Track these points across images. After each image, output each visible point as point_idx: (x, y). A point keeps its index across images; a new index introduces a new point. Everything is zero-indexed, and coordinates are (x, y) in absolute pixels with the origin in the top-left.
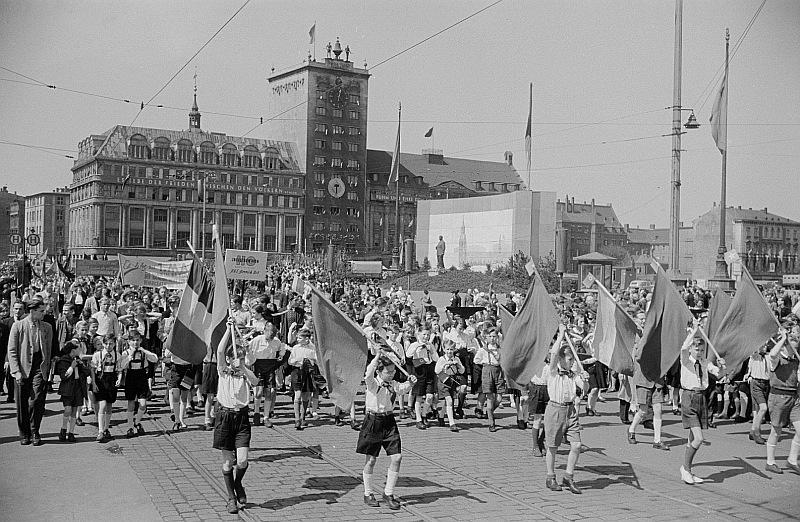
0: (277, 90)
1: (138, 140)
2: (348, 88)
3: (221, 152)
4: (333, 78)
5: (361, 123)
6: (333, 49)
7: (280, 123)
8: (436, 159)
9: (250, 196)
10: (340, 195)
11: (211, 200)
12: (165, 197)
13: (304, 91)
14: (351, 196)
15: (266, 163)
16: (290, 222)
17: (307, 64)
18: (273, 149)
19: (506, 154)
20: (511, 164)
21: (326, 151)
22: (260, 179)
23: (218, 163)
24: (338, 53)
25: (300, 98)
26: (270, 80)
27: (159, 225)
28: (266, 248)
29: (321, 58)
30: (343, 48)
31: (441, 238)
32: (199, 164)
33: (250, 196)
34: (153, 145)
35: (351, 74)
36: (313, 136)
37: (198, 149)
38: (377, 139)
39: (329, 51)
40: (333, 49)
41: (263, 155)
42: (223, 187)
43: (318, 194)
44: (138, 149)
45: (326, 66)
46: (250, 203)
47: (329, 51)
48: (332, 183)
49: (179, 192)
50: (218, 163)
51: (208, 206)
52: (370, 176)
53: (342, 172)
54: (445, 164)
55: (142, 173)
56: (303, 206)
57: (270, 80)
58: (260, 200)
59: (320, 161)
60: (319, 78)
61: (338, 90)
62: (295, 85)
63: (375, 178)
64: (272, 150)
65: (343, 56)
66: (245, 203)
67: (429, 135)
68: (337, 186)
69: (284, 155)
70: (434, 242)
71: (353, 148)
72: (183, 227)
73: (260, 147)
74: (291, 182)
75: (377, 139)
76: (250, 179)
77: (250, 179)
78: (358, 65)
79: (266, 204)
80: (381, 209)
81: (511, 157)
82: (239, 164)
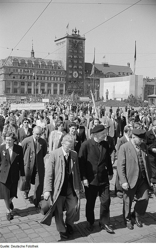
0: (57, 44)
1: (15, 60)
2: (79, 43)
3: (40, 64)
4: (74, 40)
5: (83, 54)
6: (74, 31)
8: (106, 65)
9: (49, 77)
10: (77, 77)
11: (38, 79)
12: (24, 78)
13: (65, 44)
14: (80, 77)
15: (53, 67)
16: (61, 85)
17: (66, 36)
18: (56, 63)
20: (129, 67)
21: (73, 64)
22: (52, 72)
23: (40, 67)
24: (76, 32)
25: (64, 47)
26: (55, 41)
27: (22, 87)
28: (54, 93)
29: (70, 34)
30: (77, 30)
31: (107, 90)
32: (34, 68)
33: (49, 77)
34: (20, 62)
35: (80, 39)
36: (68, 59)
37: (34, 63)
38: (88, 59)
39: (73, 32)
40: (74, 31)
41: (53, 65)
42: (41, 75)
43: (70, 77)
44: (15, 64)
46: (49, 80)
47: (73, 32)
48: (74, 73)
49: (28, 77)
50: (40, 67)
51: (37, 81)
52: (86, 71)
53: (77, 69)
54: (109, 67)
55: (17, 71)
56: (65, 81)
57: (55, 41)
58: (52, 79)
59: (70, 66)
60: (70, 40)
61: (76, 44)
62: (63, 43)
63: (87, 72)
64: (56, 63)
65: (77, 33)
66: (48, 79)
67: (104, 57)
68: (75, 74)
69: (59, 64)
70: (105, 91)
71: (80, 62)
72: (29, 87)
73: (52, 62)
74: (62, 73)
75: (88, 59)
76: (49, 72)
77: (49, 72)
78: (82, 36)
79: (54, 80)
80: (89, 81)
81: (129, 64)
82: (46, 68)
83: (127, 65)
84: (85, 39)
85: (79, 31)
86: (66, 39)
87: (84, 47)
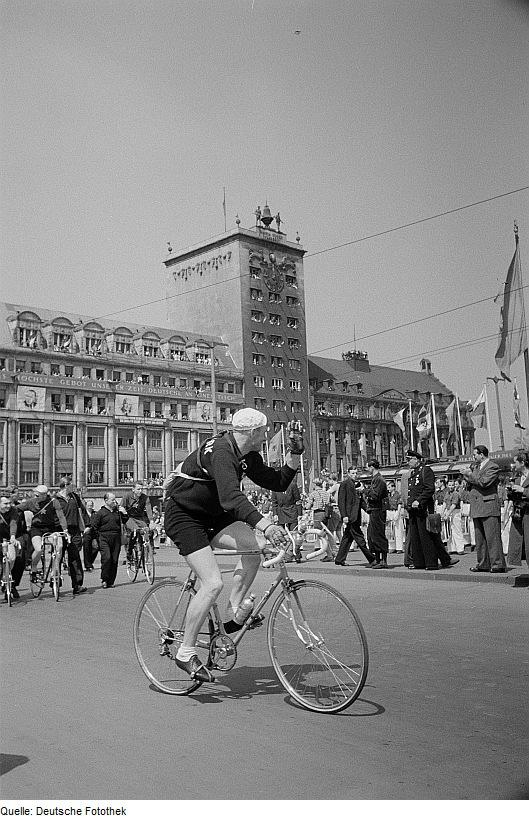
0: (183, 274)
4: (265, 250)
7: (214, 310)
17: (236, 231)
19: (423, 362)
24: (267, 221)
26: (168, 263)
27: (63, 451)
29: (250, 225)
30: (273, 214)
35: (285, 249)
37: (111, 339)
45: (257, 235)
47: (258, 218)
57: (168, 263)
65: (273, 225)
72: (95, 453)
78: (289, 240)
81: (429, 365)
83: (418, 369)
84: (304, 252)
85: (278, 221)
86: (235, 245)
87: (302, 281)
